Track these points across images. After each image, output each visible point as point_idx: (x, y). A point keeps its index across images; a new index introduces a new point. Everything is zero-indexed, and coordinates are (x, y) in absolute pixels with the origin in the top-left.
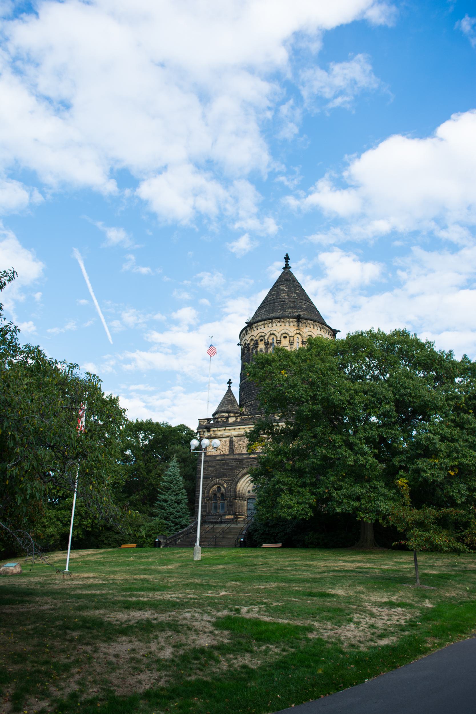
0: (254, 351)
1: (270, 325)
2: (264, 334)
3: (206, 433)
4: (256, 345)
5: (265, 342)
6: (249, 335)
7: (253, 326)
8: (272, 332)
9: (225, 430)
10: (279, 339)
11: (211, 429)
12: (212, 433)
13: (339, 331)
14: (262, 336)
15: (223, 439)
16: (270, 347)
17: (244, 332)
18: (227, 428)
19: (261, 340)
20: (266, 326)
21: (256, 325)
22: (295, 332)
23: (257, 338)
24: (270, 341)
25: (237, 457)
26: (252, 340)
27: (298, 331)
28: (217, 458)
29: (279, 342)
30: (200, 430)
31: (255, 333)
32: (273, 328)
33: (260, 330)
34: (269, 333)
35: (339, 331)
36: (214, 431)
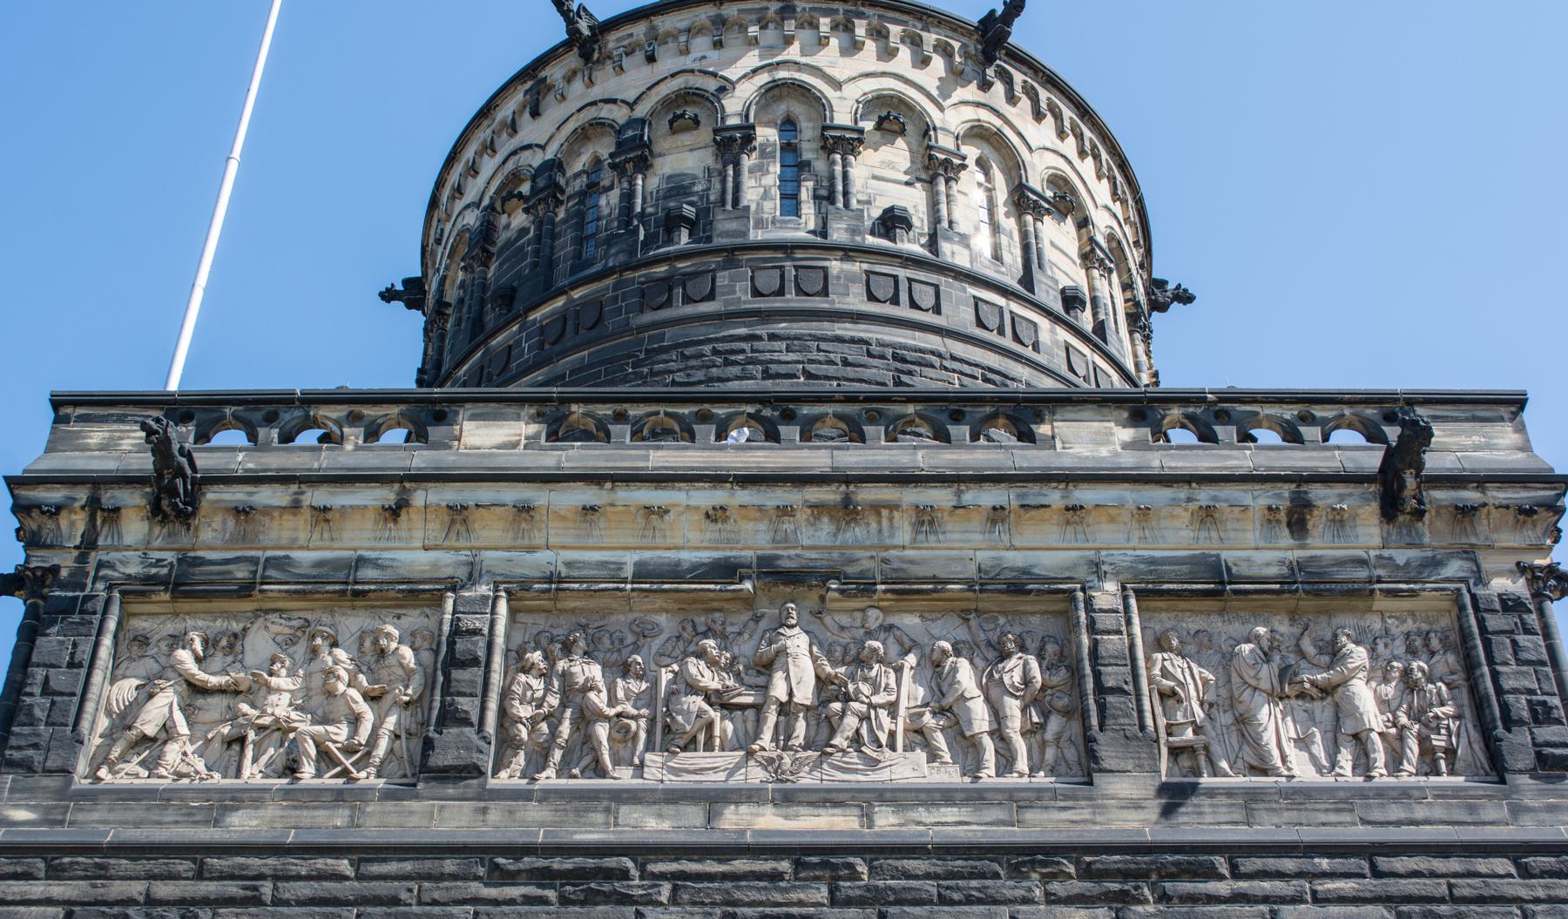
0: (609, 202)
1: (770, 36)
2: (711, 85)
3: (134, 528)
4: (634, 152)
5: (716, 132)
6: (554, 112)
7: (612, 40)
8: (782, 74)
9: (394, 512)
10: (843, 117)
11: (212, 495)
12: (211, 536)
13: (1185, 297)
14: (690, 96)
15: (352, 623)
16: (760, 170)
17: (505, 111)
18: (419, 498)
19: (678, 125)
20: (732, 38)
21: (639, 30)
22: (970, 113)
23: (641, 110)
24: (767, 134)
25: (534, 824)
26: (598, 125)
27: (985, 115)
28: (242, 825)
29: (843, 143)
30: (55, 495)
31: (630, 84)
32: (793, 52)
33: (668, 62)
34: (764, 78)
35: (1185, 297)
36: (243, 512)
